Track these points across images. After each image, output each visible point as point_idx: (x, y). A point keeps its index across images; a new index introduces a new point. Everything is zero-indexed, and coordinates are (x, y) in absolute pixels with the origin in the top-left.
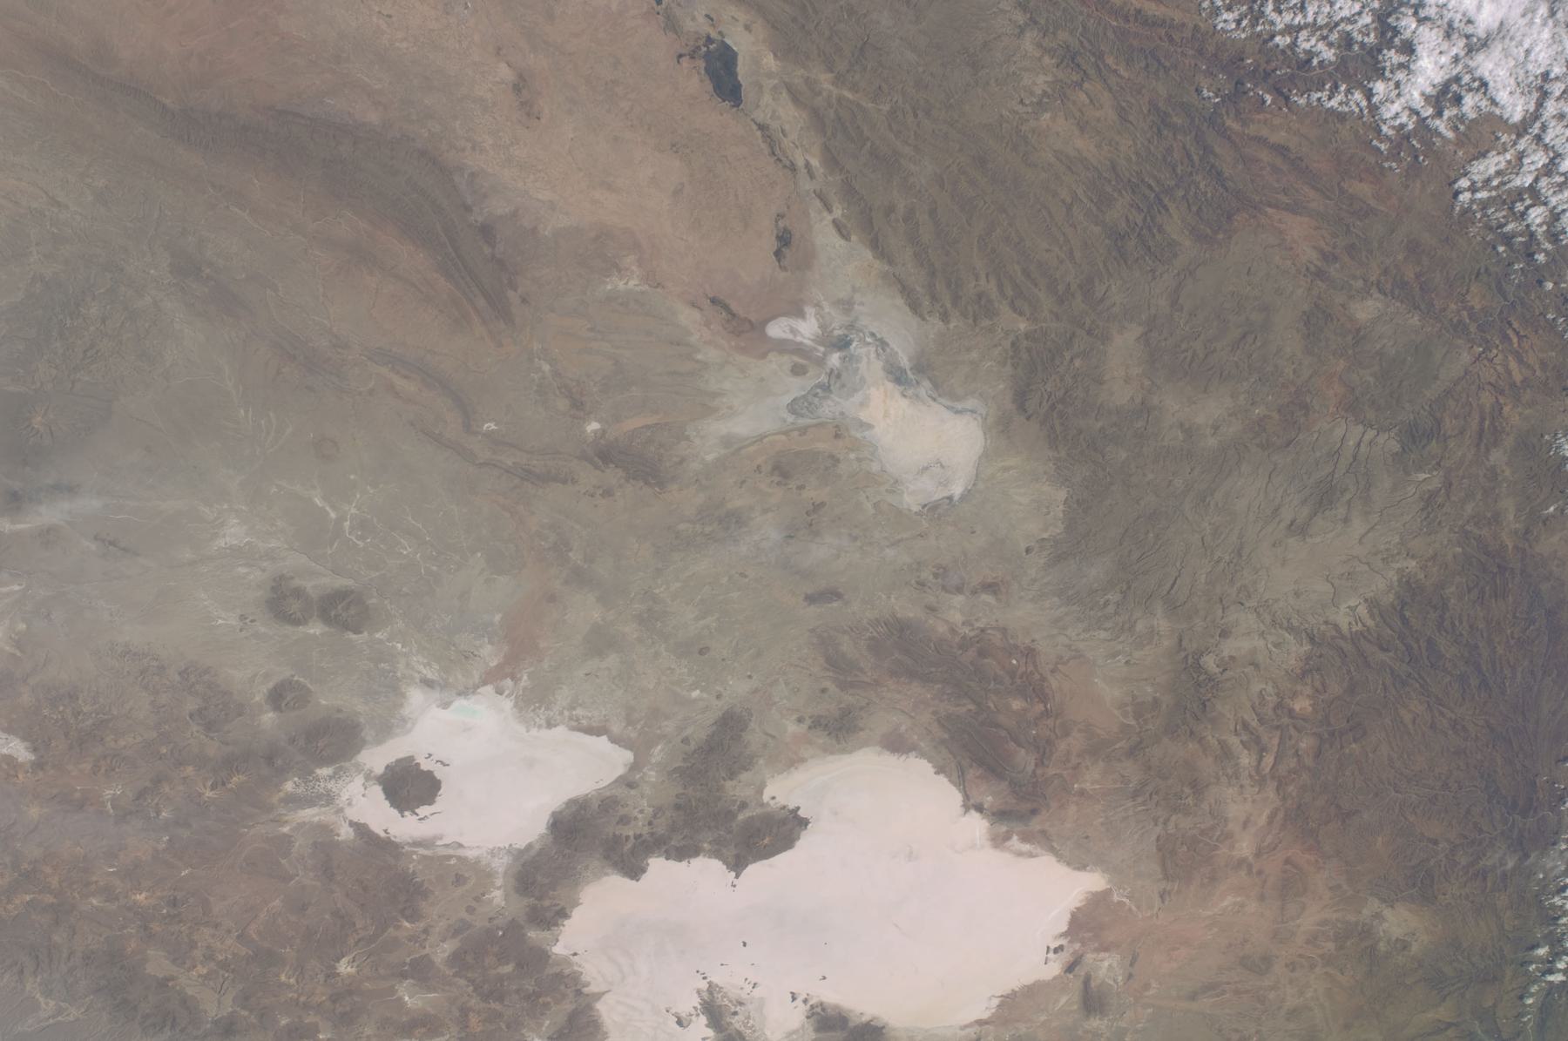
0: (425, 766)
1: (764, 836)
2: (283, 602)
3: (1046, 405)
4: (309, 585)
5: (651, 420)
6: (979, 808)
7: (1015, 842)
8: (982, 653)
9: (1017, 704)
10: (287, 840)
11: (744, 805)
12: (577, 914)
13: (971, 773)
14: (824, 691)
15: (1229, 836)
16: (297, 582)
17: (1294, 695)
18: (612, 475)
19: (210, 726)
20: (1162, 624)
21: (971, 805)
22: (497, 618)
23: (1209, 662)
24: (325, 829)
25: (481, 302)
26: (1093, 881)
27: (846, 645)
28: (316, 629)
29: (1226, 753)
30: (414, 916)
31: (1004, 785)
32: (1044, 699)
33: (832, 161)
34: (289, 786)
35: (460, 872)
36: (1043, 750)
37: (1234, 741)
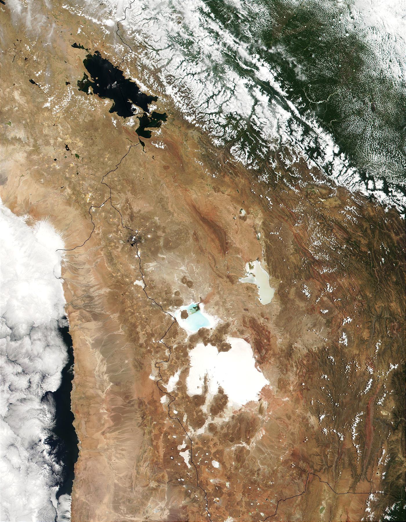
1: (225, 348)
3: (281, 295)
4: (188, 279)
6: (255, 358)
7: (258, 367)
8: (263, 329)
12: (195, 348)
13: (256, 351)
15: (289, 384)
17: (304, 360)
18: (228, 280)
19: (166, 294)
20: (288, 336)
23: (293, 346)
26: (267, 382)
27: (246, 319)
28: (185, 285)
29: (292, 366)
30: (174, 338)
32: (269, 342)
33: (266, 251)
35: (183, 333)
36: (267, 350)
37: (294, 364)
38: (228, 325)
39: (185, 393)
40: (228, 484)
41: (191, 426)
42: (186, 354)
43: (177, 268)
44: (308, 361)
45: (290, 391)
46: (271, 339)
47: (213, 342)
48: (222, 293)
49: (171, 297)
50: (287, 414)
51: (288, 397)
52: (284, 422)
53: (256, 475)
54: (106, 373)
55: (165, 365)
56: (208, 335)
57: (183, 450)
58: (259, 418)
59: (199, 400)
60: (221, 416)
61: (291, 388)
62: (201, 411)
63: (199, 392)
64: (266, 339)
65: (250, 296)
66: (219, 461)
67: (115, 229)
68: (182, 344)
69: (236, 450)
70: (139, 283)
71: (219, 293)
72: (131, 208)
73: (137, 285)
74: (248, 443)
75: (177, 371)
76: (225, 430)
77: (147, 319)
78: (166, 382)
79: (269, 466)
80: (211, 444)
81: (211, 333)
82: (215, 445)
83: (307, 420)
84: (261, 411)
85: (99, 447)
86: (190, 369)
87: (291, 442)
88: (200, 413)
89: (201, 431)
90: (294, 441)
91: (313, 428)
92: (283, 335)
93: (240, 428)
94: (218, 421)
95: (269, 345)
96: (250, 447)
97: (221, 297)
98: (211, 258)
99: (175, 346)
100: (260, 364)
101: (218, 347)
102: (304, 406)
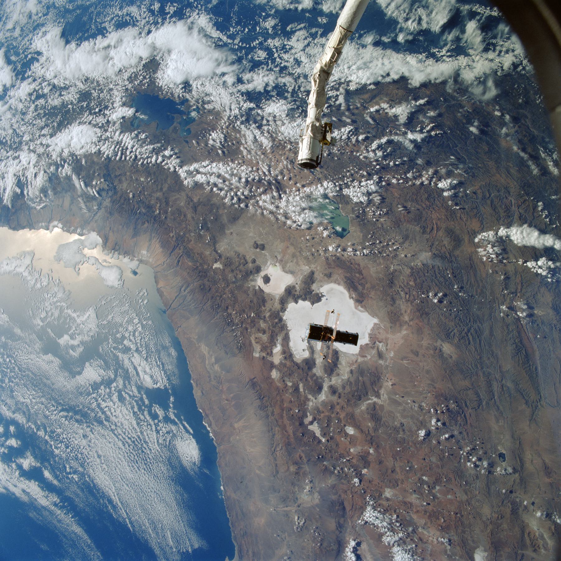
0: (269, 276)
2: (256, 246)
7: (360, 308)
10: (249, 288)
11: (313, 291)
12: (287, 310)
13: (351, 290)
15: (402, 314)
21: (351, 297)
24: (254, 286)
26: (376, 321)
30: (264, 306)
32: (362, 275)
35: (272, 298)
36: (363, 285)
37: (400, 290)
38: (312, 273)
39: (293, 361)
40: (371, 451)
41: (310, 394)
42: (281, 320)
44: (415, 280)
45: (406, 322)
46: (364, 272)
50: (412, 351)
51: (406, 329)
52: (412, 361)
53: (401, 433)
54: (216, 364)
55: (265, 338)
56: (296, 291)
57: (311, 423)
58: (381, 364)
60: (338, 375)
61: (406, 318)
62: (315, 375)
63: (307, 355)
66: (353, 427)
67: (184, 226)
68: (273, 310)
69: (367, 409)
70: (217, 265)
71: (292, 244)
72: (192, 201)
73: (216, 268)
74: (378, 396)
75: (277, 340)
76: (348, 389)
78: (271, 354)
79: (412, 417)
80: (338, 408)
81: (298, 288)
82: (342, 408)
83: (440, 350)
84: (380, 355)
85: (231, 439)
86: (290, 333)
87: (429, 382)
88: (315, 378)
89: (322, 397)
90: (433, 380)
91: (451, 357)
92: (375, 261)
93: (364, 382)
94: (335, 381)
96: (382, 399)
99: (268, 315)
100: (361, 303)
101: (310, 301)
102: (429, 334)
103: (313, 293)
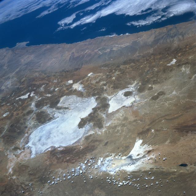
5: (147, 137)
6: (59, 148)
7: (50, 149)
9: (68, 158)
13: (65, 149)
14: (94, 138)
16: (163, 95)
18: (145, 129)
22: (139, 111)
24: (132, 84)
25: (179, 127)
27: (97, 143)
30: (112, 87)
31: (59, 151)
32: (65, 162)
34: (140, 84)
36: (58, 159)
42: (94, 95)
43: (176, 88)
47: (93, 115)
48: (134, 123)
49: (150, 84)
55: (94, 82)
59: (54, 103)
64: (69, 159)
65: (118, 148)
76: (22, 121)
77: (138, 69)
89: (33, 105)
95: (63, 161)
97: (130, 123)
98: (175, 116)
99: (105, 88)
103: (88, 122)
